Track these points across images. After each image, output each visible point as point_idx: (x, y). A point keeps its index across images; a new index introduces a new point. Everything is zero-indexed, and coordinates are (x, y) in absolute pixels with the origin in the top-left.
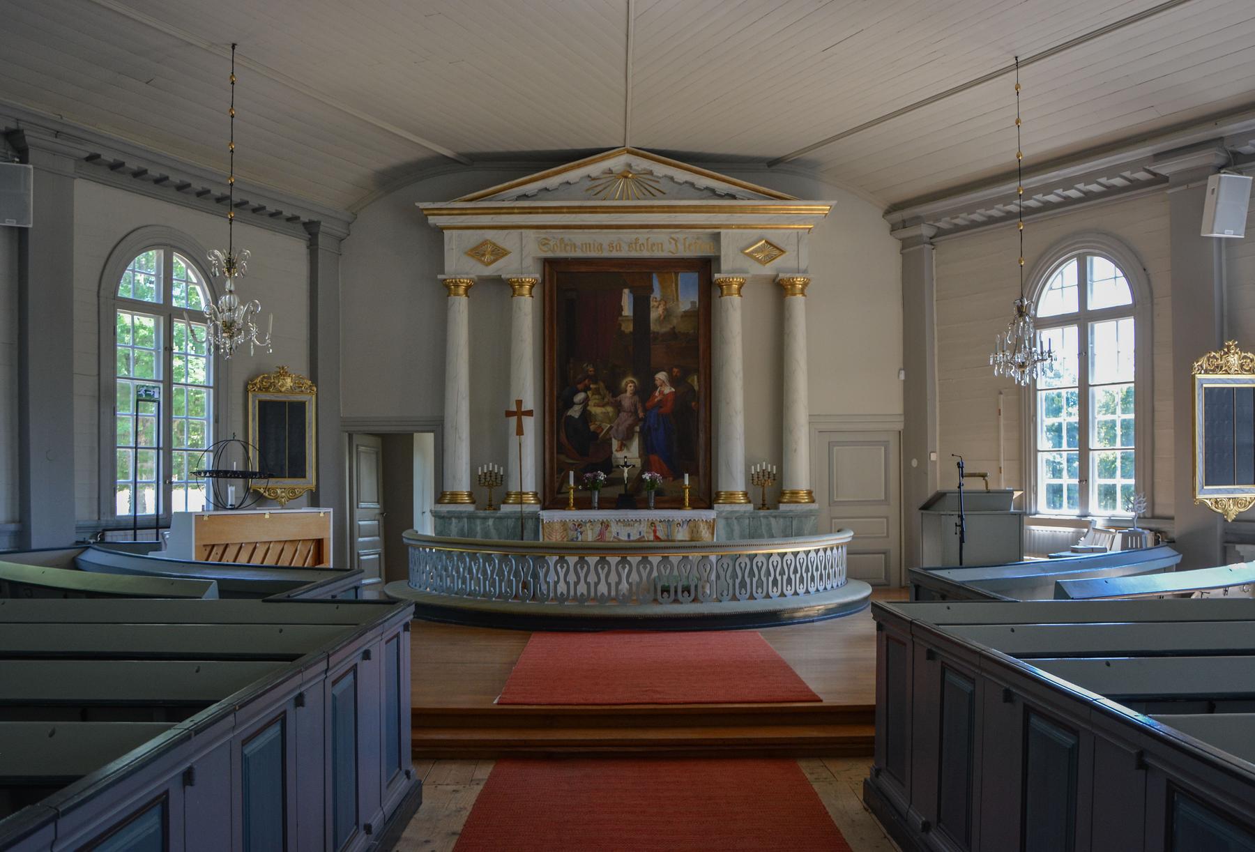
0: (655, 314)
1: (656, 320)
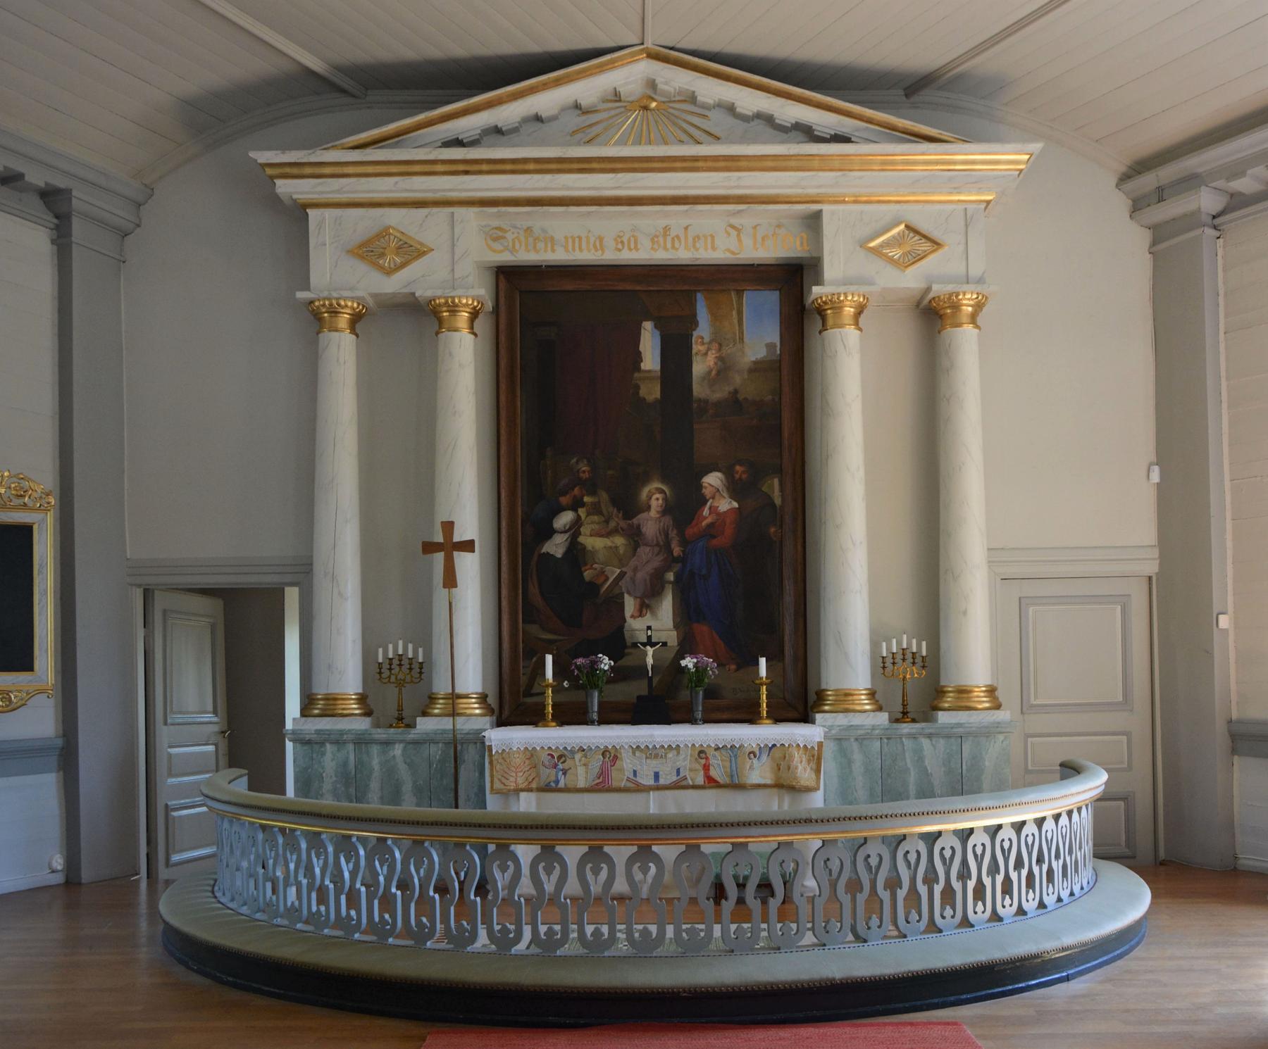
0: (700, 367)
1: (703, 379)
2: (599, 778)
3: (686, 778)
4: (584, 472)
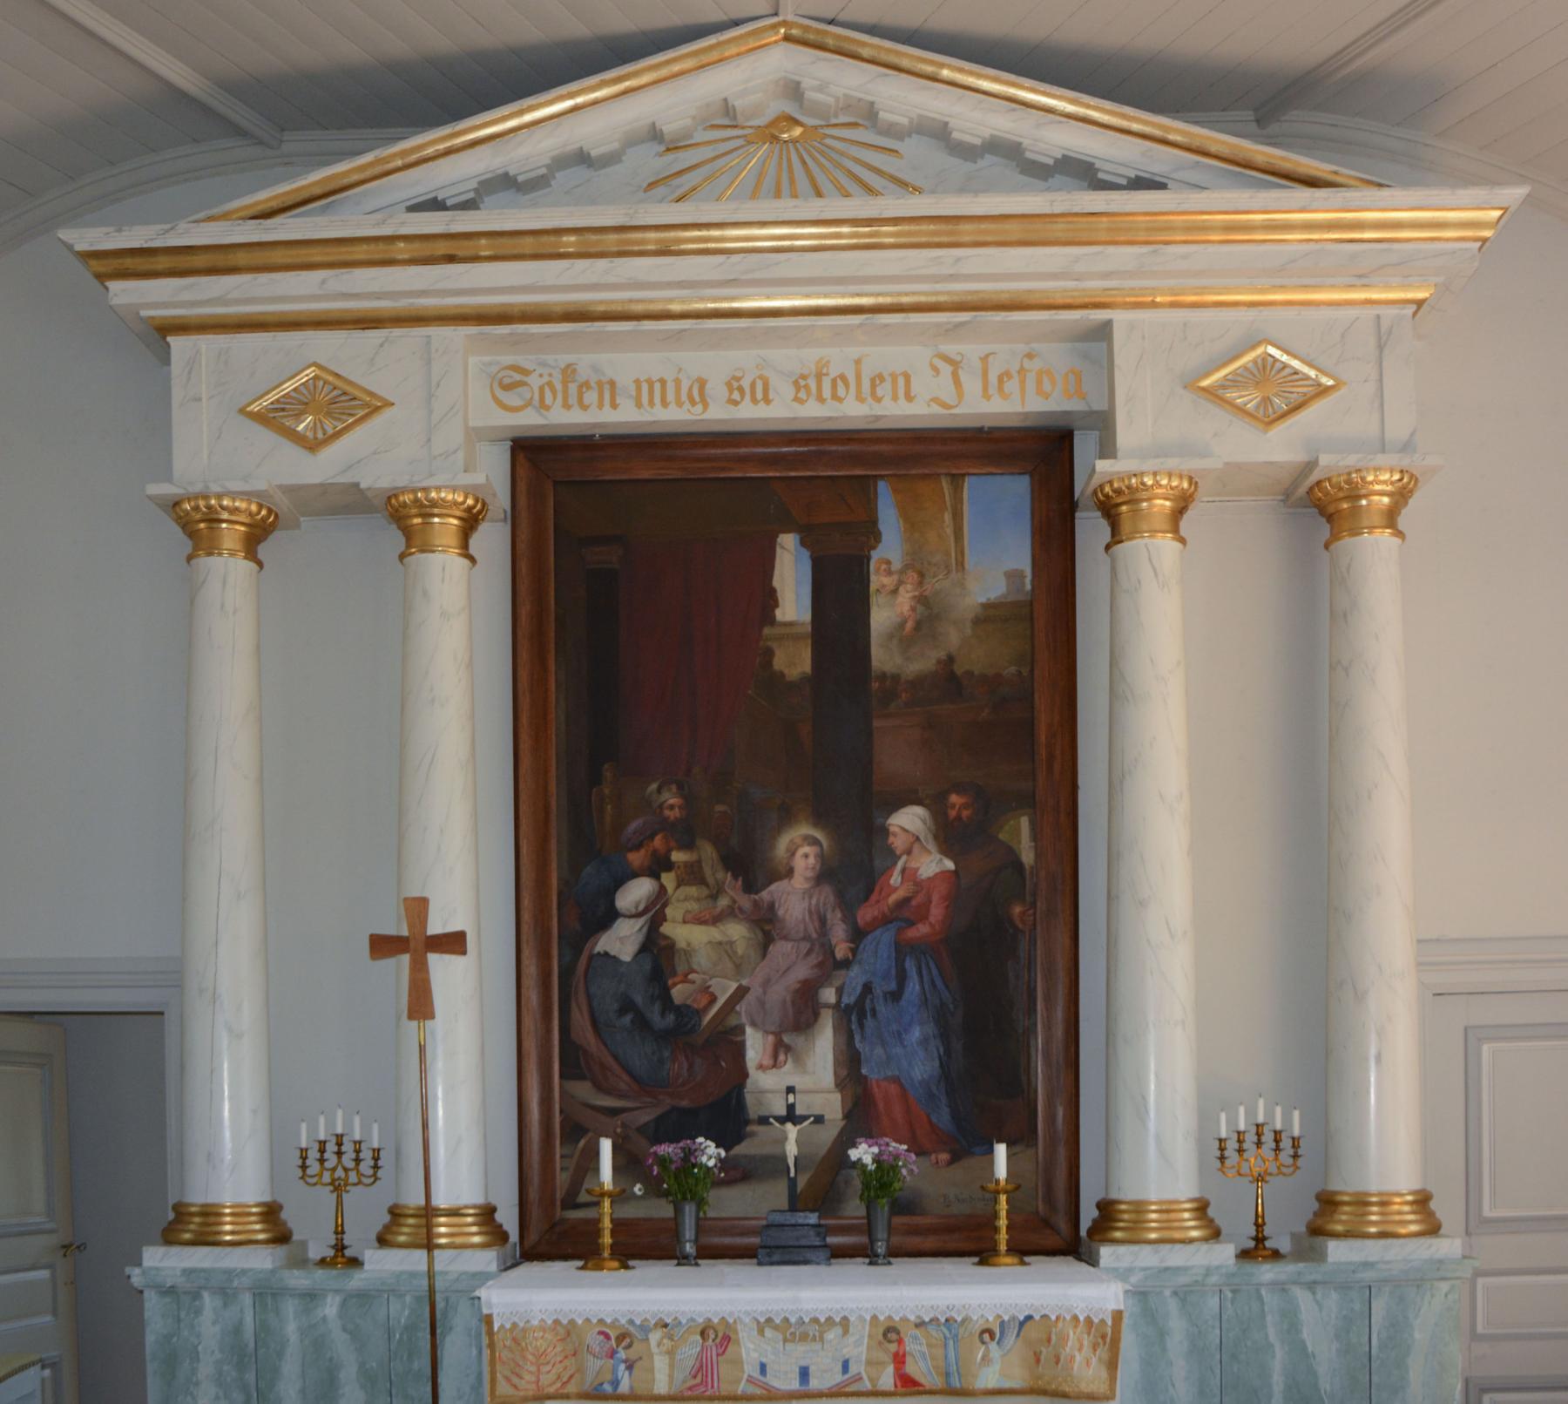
0: (883, 616)
1: (891, 636)
2: (695, 1377)
3: (861, 1378)
4: (672, 807)
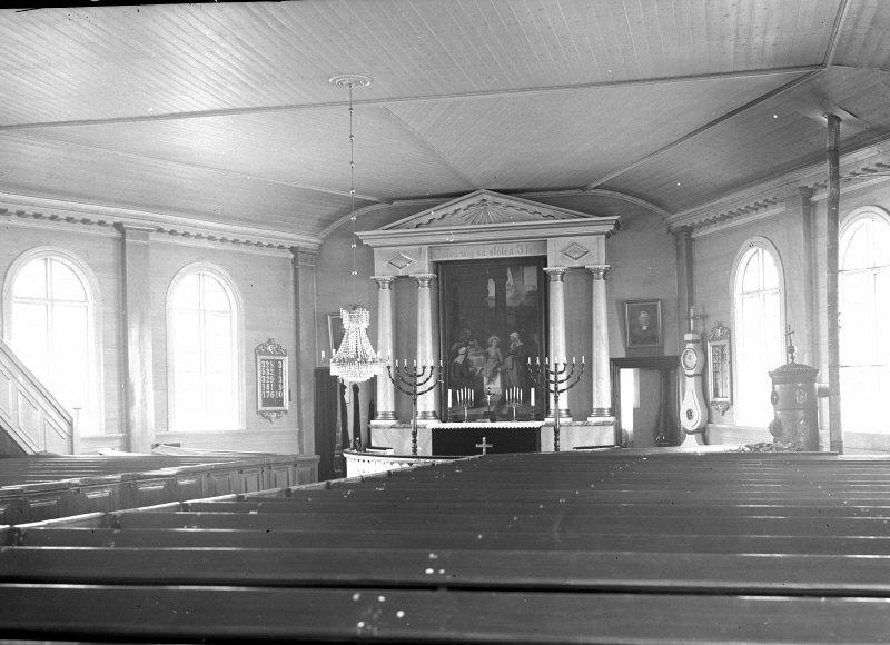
0: (509, 295)
